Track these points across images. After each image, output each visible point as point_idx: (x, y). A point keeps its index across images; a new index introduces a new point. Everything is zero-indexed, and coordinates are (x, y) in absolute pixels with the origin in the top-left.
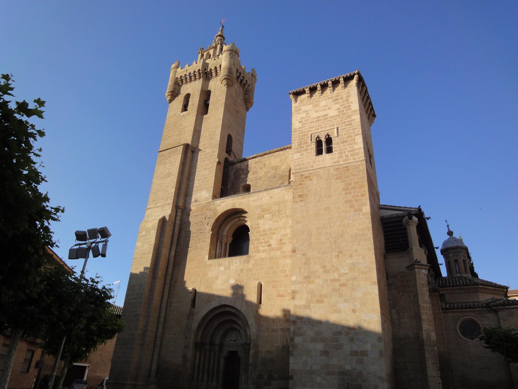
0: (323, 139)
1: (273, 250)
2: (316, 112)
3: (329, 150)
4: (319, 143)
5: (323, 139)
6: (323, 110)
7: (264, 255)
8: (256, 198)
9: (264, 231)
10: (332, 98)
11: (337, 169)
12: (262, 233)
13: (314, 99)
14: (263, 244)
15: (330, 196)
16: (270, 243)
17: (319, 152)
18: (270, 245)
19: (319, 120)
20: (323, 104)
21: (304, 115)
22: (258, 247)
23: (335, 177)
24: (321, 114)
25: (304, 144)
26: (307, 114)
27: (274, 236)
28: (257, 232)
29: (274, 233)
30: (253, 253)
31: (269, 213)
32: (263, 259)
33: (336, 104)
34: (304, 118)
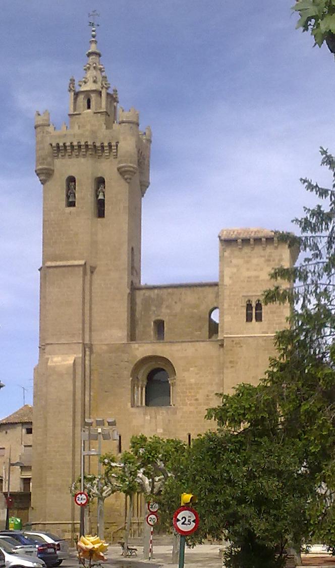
0: (254, 305)
1: (199, 404)
2: (248, 270)
3: (259, 318)
4: (249, 307)
5: (254, 305)
6: (255, 270)
7: (192, 409)
8: (179, 347)
9: (191, 384)
10: (264, 256)
11: (265, 340)
12: (188, 387)
13: (246, 253)
14: (190, 397)
15: (258, 366)
16: (197, 397)
17: (249, 319)
18: (197, 400)
19: (250, 282)
20: (255, 261)
21: (235, 270)
22: (185, 400)
23: (263, 348)
24: (253, 273)
25: (235, 305)
26: (238, 270)
27: (200, 391)
28: (183, 385)
29: (201, 388)
30: (180, 406)
31: (196, 366)
32: (191, 412)
33: (268, 265)
34: (235, 274)
